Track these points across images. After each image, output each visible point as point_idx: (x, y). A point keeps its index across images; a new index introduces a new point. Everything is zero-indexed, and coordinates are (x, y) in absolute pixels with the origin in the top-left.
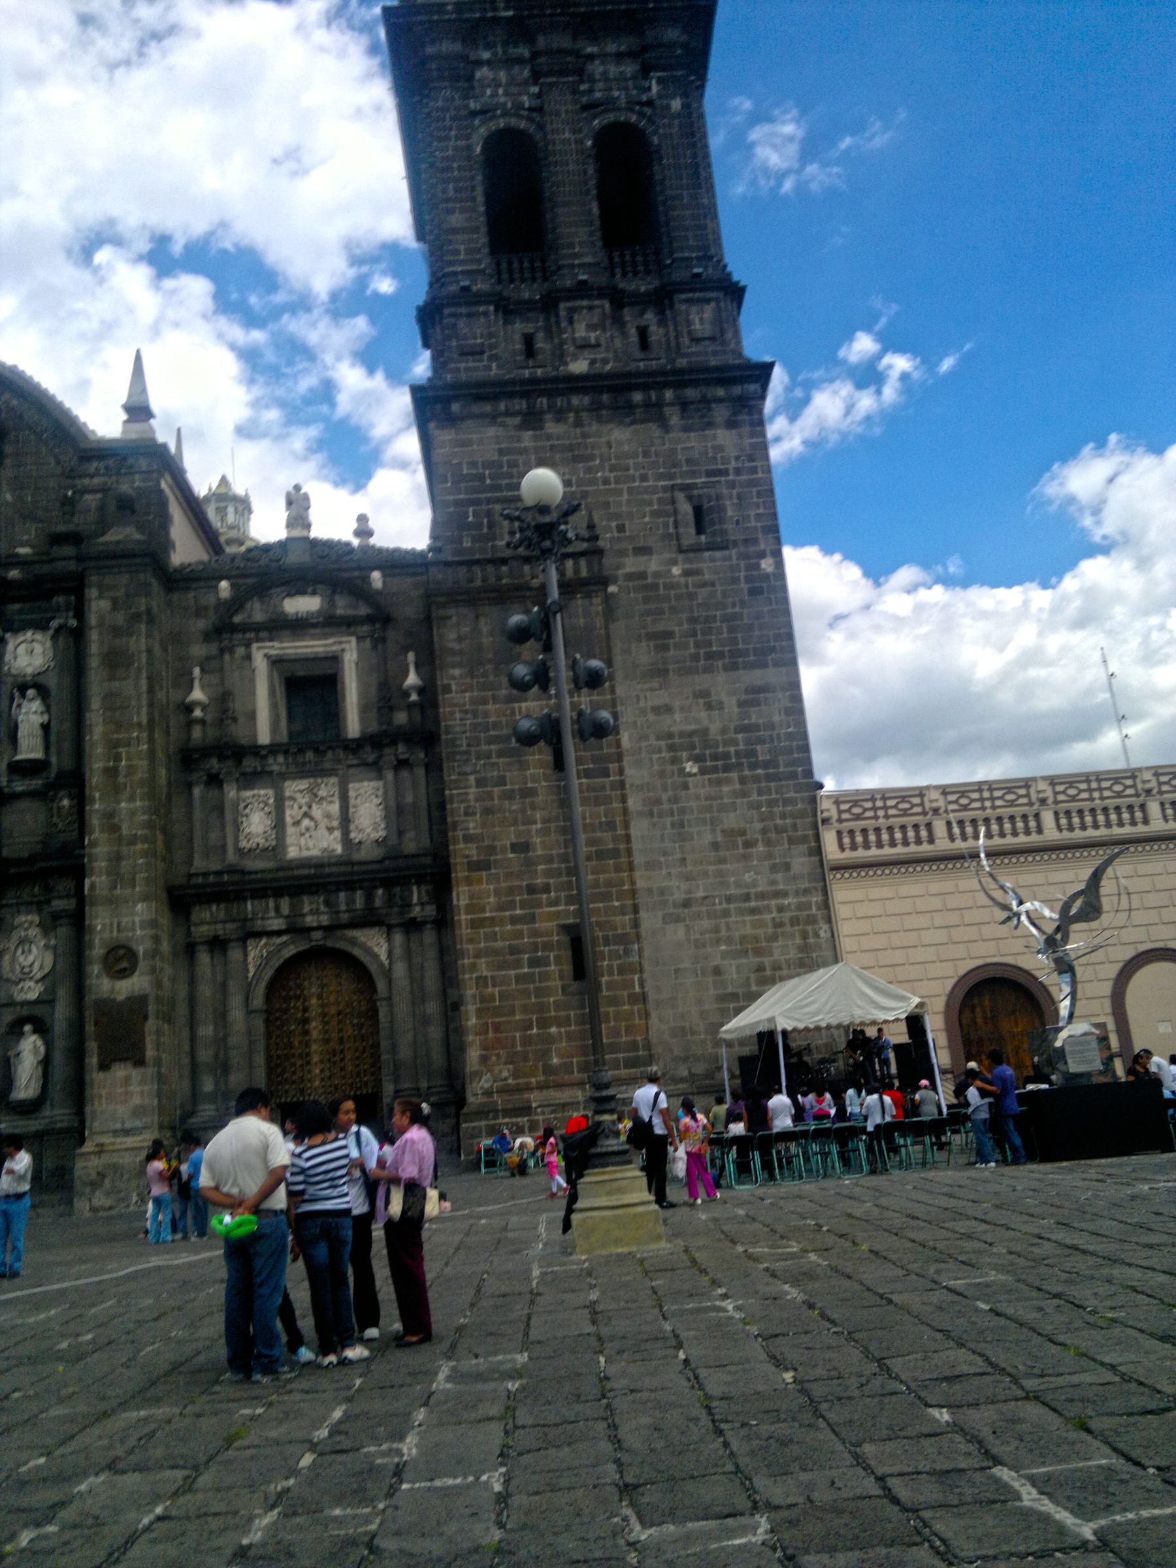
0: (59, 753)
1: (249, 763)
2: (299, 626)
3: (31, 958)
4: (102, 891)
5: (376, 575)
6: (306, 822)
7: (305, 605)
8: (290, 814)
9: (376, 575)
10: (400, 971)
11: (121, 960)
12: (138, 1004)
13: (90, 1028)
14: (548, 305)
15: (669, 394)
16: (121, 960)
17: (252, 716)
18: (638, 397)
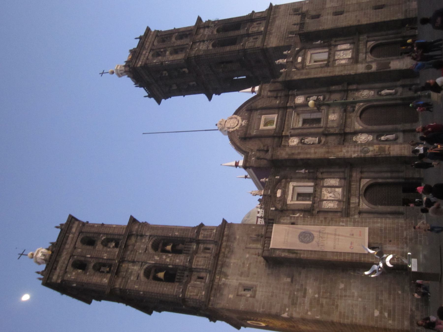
2: (304, 60)
5: (297, 49)
7: (300, 59)
8: (341, 58)
9: (297, 49)
10: (376, 38)
11: (369, 67)
13: (382, 70)
14: (248, 35)
15: (271, 17)
17: (321, 64)
18: (270, 21)
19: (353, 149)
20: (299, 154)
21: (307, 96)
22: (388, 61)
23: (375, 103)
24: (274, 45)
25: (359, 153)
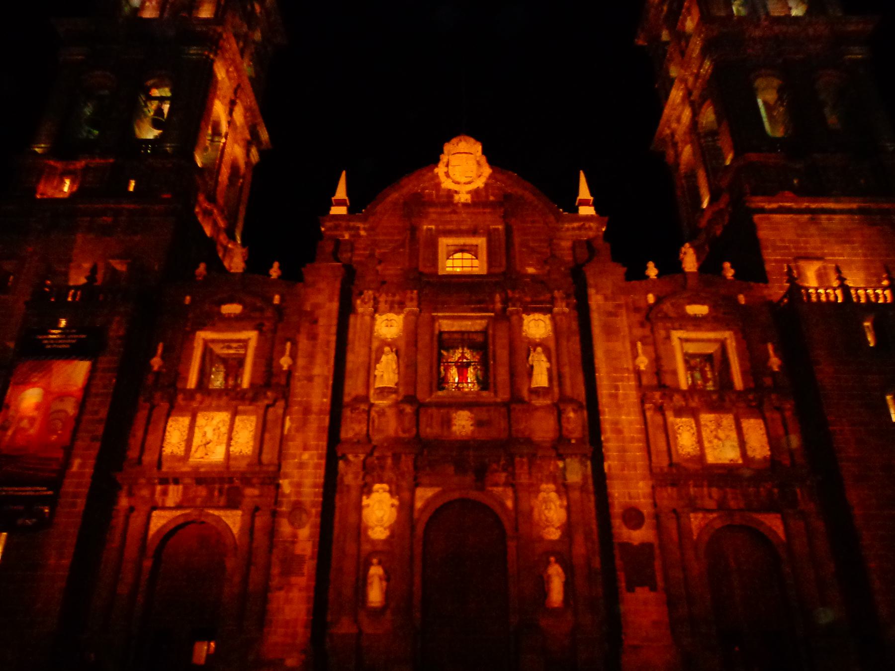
0: (561, 385)
1: (678, 400)
3: (552, 512)
4: (613, 472)
6: (715, 441)
8: (705, 434)
12: (646, 547)
13: (618, 562)
16: (633, 517)
17: (675, 373)
19: (308, 481)
20: (313, 337)
21: (552, 345)
22: (660, 584)
23: (512, 544)
24: (764, 233)
25: (293, 498)
